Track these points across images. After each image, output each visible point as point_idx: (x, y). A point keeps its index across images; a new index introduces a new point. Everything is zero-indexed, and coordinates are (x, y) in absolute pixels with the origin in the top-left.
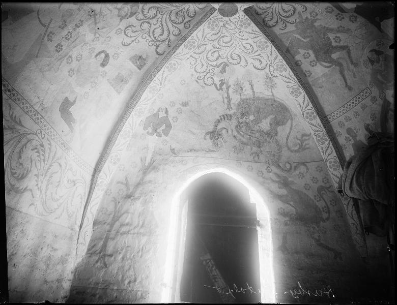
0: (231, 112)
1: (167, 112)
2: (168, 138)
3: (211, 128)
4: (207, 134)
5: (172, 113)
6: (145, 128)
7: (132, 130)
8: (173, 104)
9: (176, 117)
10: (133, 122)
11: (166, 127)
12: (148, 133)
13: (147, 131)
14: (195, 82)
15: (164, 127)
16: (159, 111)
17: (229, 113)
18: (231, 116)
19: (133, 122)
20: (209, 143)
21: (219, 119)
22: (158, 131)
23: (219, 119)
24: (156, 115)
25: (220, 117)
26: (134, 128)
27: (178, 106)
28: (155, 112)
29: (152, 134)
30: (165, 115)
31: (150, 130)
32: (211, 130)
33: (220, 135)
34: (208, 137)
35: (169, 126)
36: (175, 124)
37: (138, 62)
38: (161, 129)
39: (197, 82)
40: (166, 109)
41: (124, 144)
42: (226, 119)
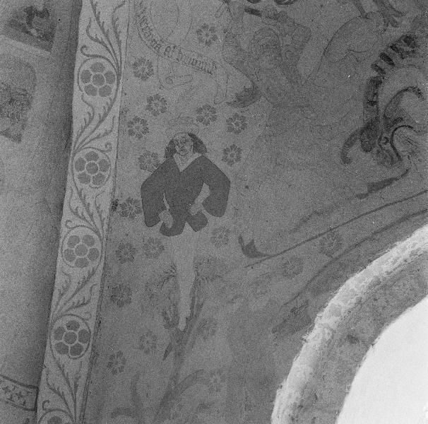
0: (405, 27)
1: (197, 145)
2: (225, 221)
3: (357, 120)
4: (349, 143)
5: (215, 139)
6: (151, 221)
7: (97, 232)
8: (206, 113)
9: (233, 147)
10: (87, 206)
11: (212, 189)
12: (166, 231)
13: (160, 224)
14: (247, 16)
15: (205, 192)
16: (171, 151)
17: (395, 33)
18: (409, 40)
19: (87, 206)
20: (366, 164)
21: (375, 74)
22: (194, 210)
23: (375, 74)
24: (165, 169)
25: (375, 67)
26: (99, 226)
27: (225, 113)
28: (162, 160)
29: (177, 230)
30: (197, 155)
31: (166, 218)
32: (361, 125)
33: (395, 122)
34: (356, 151)
35: (222, 185)
36: (237, 165)
37: (33, 31)
38: (200, 199)
39: (253, 12)
40: (191, 135)
41: (85, 282)
42: (396, 58)
